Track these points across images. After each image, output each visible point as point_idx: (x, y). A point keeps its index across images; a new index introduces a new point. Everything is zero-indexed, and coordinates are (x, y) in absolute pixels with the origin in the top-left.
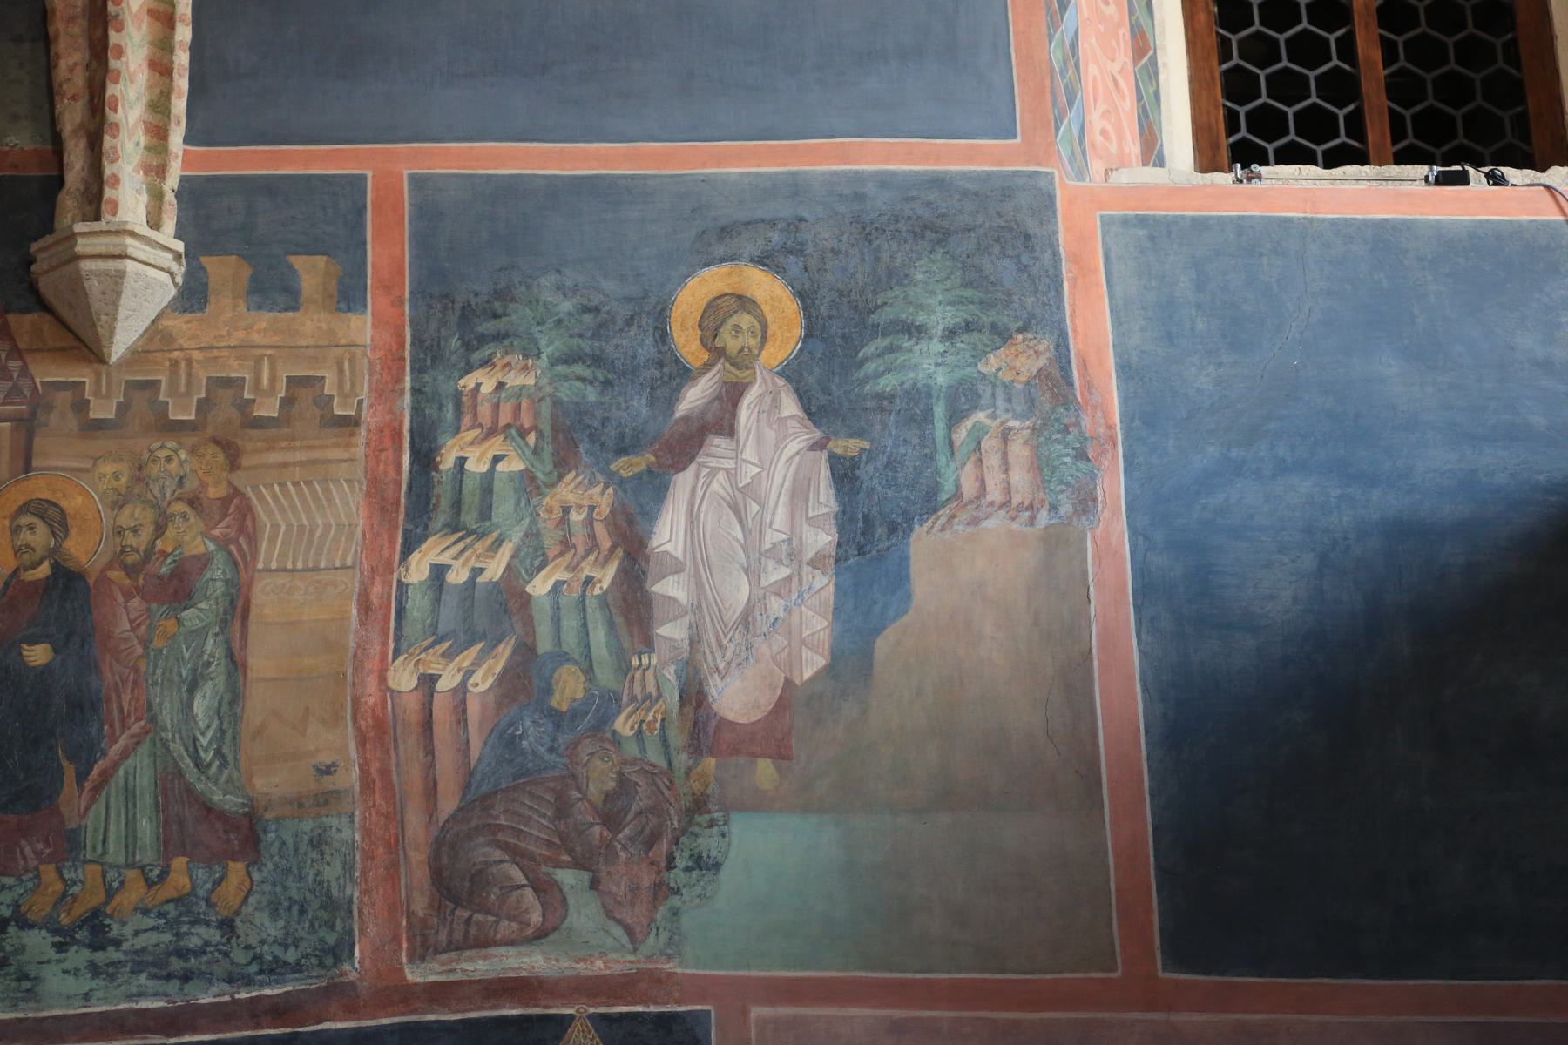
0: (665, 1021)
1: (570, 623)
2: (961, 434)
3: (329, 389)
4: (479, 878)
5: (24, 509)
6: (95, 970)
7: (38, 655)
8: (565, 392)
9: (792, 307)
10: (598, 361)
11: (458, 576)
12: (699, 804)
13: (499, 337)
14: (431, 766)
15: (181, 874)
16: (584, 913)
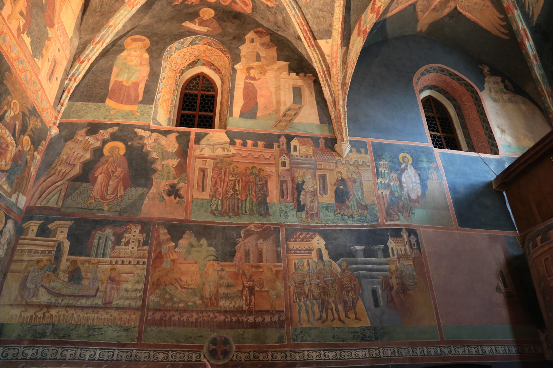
0: (412, 229)
1: (395, 188)
2: (429, 172)
3: (366, 162)
4: (391, 214)
5: (337, 172)
6: (353, 221)
7: (341, 187)
8: (390, 164)
9: (411, 158)
10: (393, 161)
11: (383, 182)
12: (411, 207)
13: (383, 158)
14: (384, 202)
15: (360, 211)
16: (402, 218)
